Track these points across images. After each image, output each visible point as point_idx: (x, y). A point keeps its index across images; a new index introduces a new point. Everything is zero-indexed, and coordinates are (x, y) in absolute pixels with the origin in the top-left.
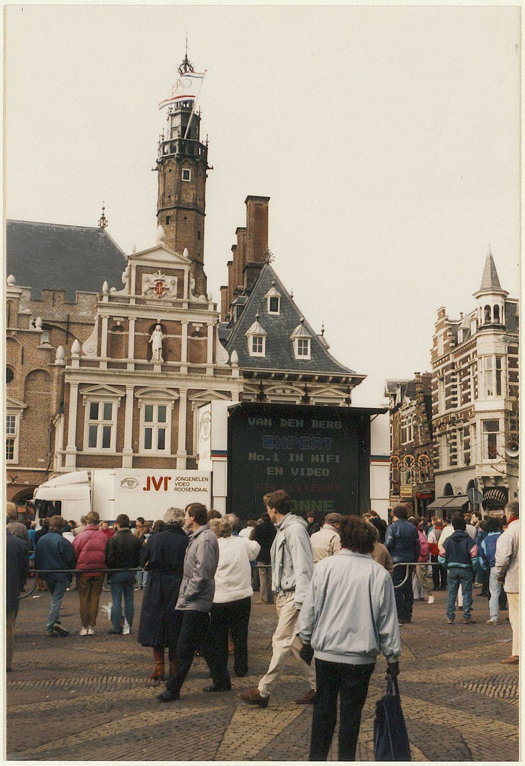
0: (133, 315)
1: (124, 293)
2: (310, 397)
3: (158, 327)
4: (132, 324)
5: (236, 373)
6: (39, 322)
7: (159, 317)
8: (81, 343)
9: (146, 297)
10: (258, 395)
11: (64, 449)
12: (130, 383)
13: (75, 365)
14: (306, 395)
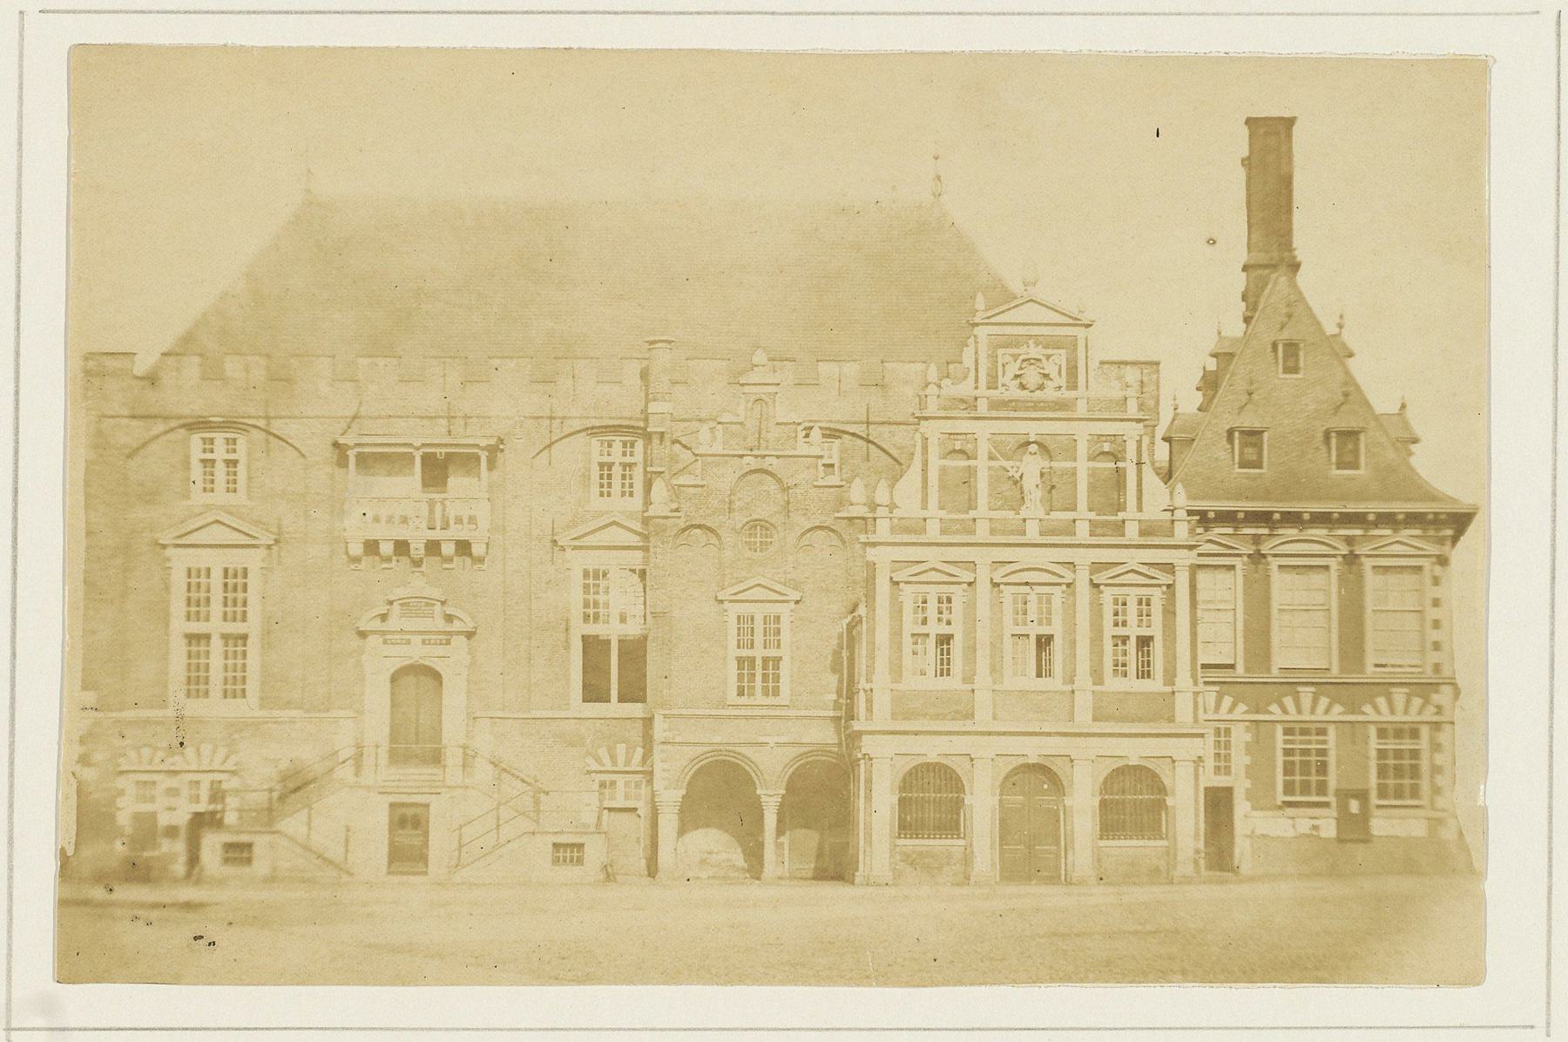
0: (982, 430)
1: (965, 389)
2: (1357, 556)
3: (1033, 448)
4: (983, 448)
5: (1182, 532)
6: (816, 434)
7: (1033, 430)
8: (892, 486)
9: (1007, 393)
10: (1249, 556)
11: (868, 680)
12: (982, 557)
13: (883, 530)
14: (1351, 552)
